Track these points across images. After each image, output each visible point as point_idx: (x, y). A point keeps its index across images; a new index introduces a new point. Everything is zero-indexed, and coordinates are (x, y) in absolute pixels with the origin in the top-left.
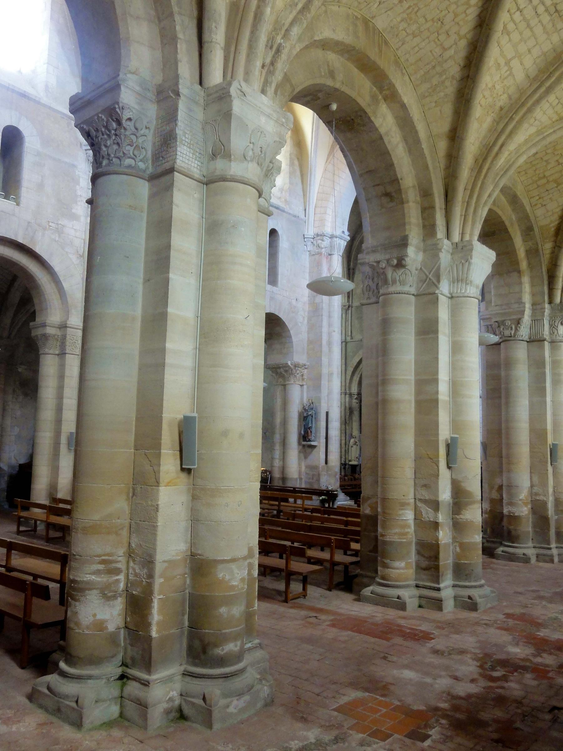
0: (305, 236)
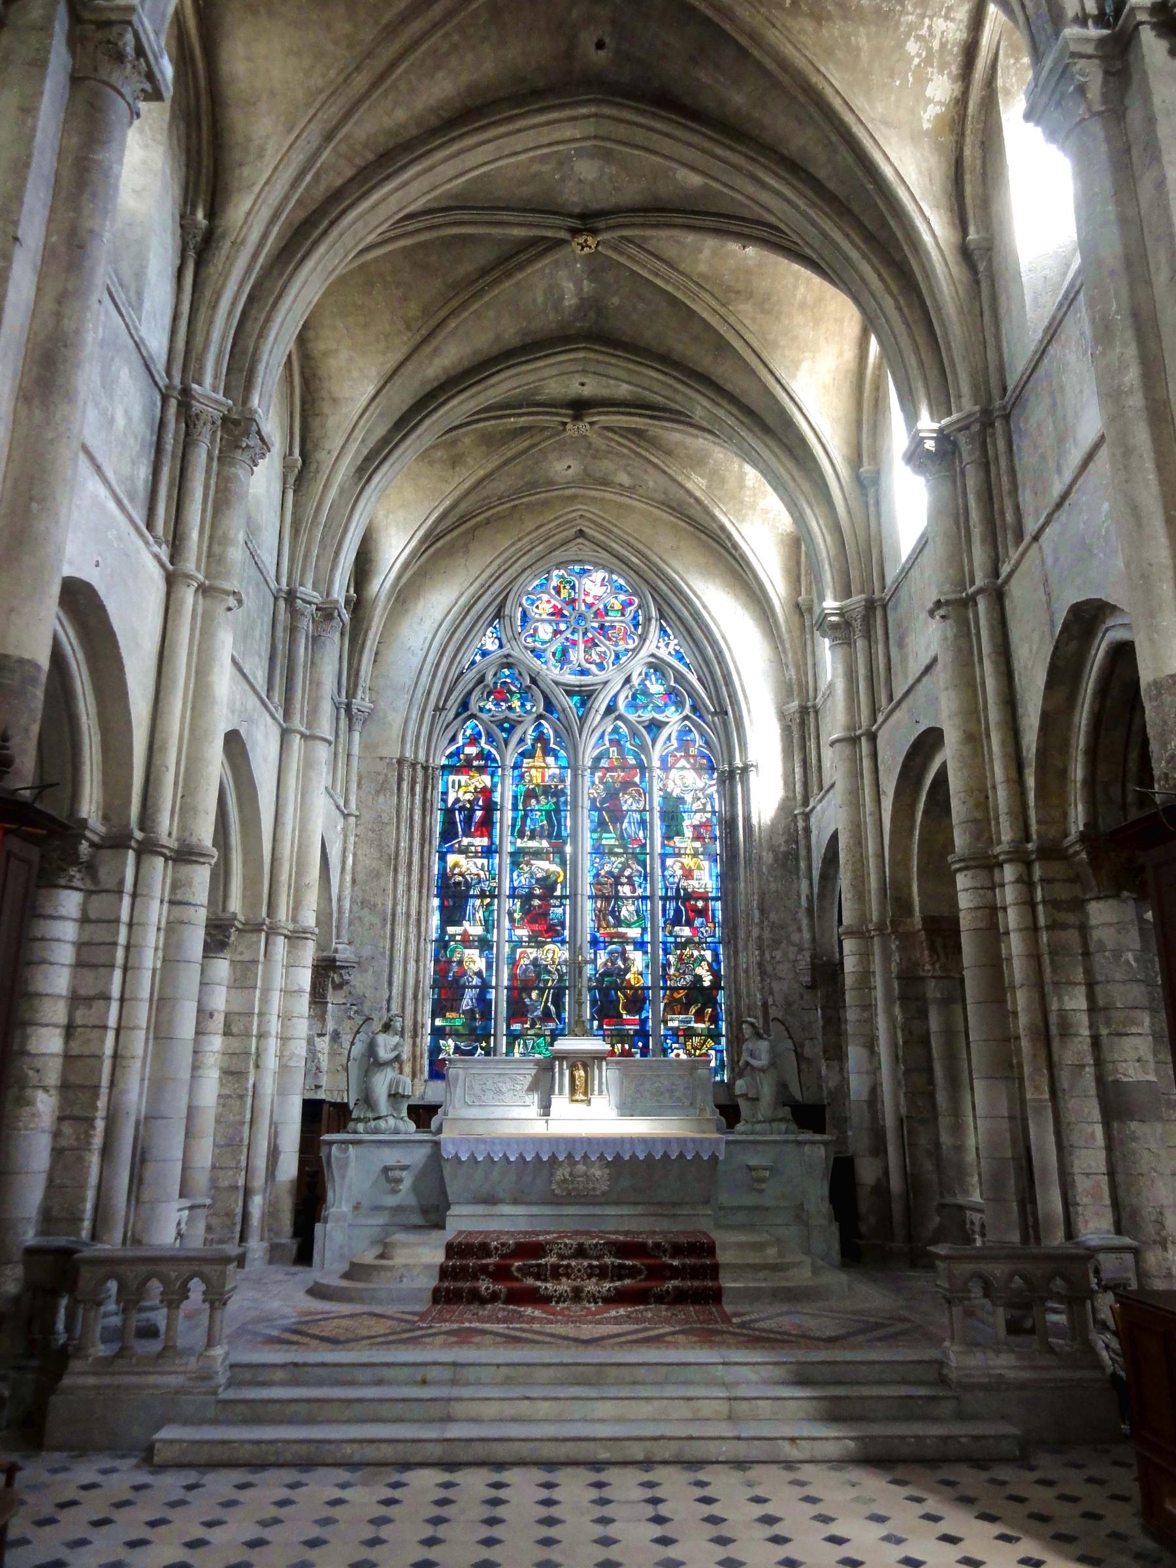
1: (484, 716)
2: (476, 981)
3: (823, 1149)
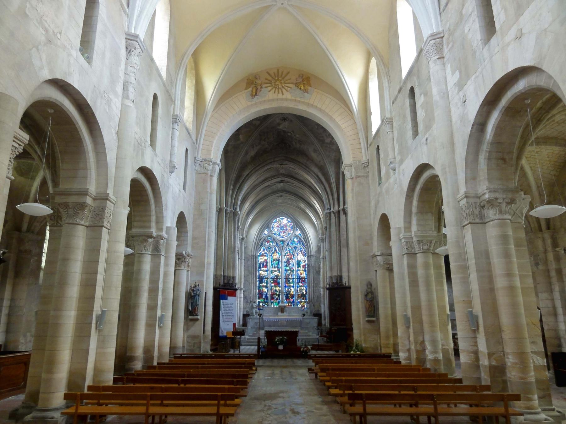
0: (196, 159)
2: (265, 293)
3: (316, 320)
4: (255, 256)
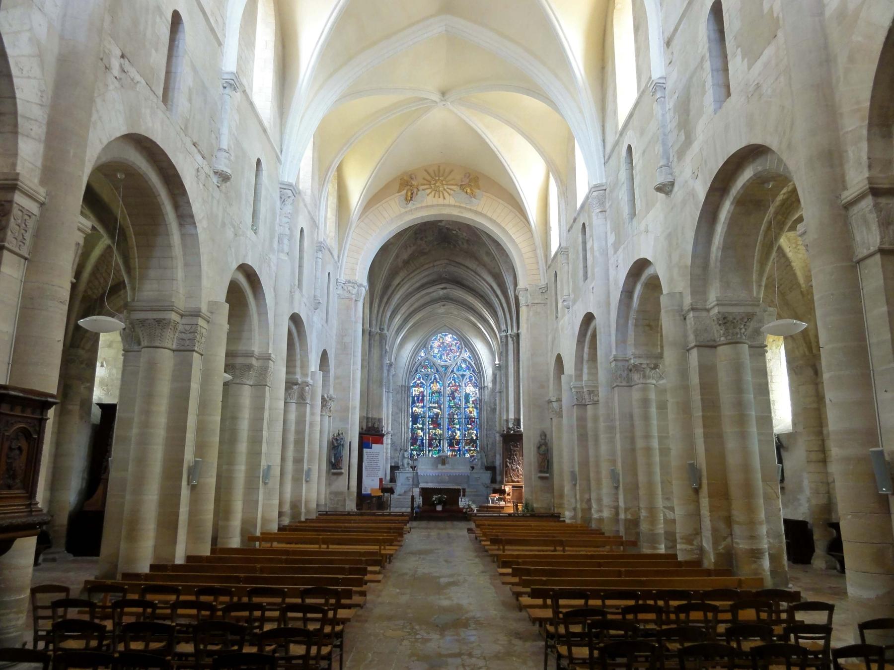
1: (422, 373)
2: (420, 438)
4: (408, 387)
